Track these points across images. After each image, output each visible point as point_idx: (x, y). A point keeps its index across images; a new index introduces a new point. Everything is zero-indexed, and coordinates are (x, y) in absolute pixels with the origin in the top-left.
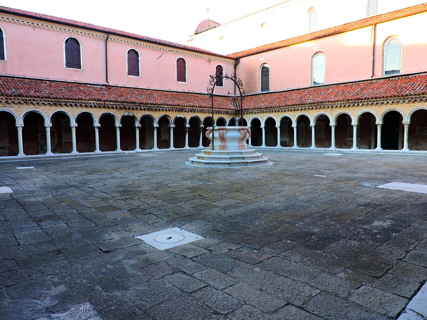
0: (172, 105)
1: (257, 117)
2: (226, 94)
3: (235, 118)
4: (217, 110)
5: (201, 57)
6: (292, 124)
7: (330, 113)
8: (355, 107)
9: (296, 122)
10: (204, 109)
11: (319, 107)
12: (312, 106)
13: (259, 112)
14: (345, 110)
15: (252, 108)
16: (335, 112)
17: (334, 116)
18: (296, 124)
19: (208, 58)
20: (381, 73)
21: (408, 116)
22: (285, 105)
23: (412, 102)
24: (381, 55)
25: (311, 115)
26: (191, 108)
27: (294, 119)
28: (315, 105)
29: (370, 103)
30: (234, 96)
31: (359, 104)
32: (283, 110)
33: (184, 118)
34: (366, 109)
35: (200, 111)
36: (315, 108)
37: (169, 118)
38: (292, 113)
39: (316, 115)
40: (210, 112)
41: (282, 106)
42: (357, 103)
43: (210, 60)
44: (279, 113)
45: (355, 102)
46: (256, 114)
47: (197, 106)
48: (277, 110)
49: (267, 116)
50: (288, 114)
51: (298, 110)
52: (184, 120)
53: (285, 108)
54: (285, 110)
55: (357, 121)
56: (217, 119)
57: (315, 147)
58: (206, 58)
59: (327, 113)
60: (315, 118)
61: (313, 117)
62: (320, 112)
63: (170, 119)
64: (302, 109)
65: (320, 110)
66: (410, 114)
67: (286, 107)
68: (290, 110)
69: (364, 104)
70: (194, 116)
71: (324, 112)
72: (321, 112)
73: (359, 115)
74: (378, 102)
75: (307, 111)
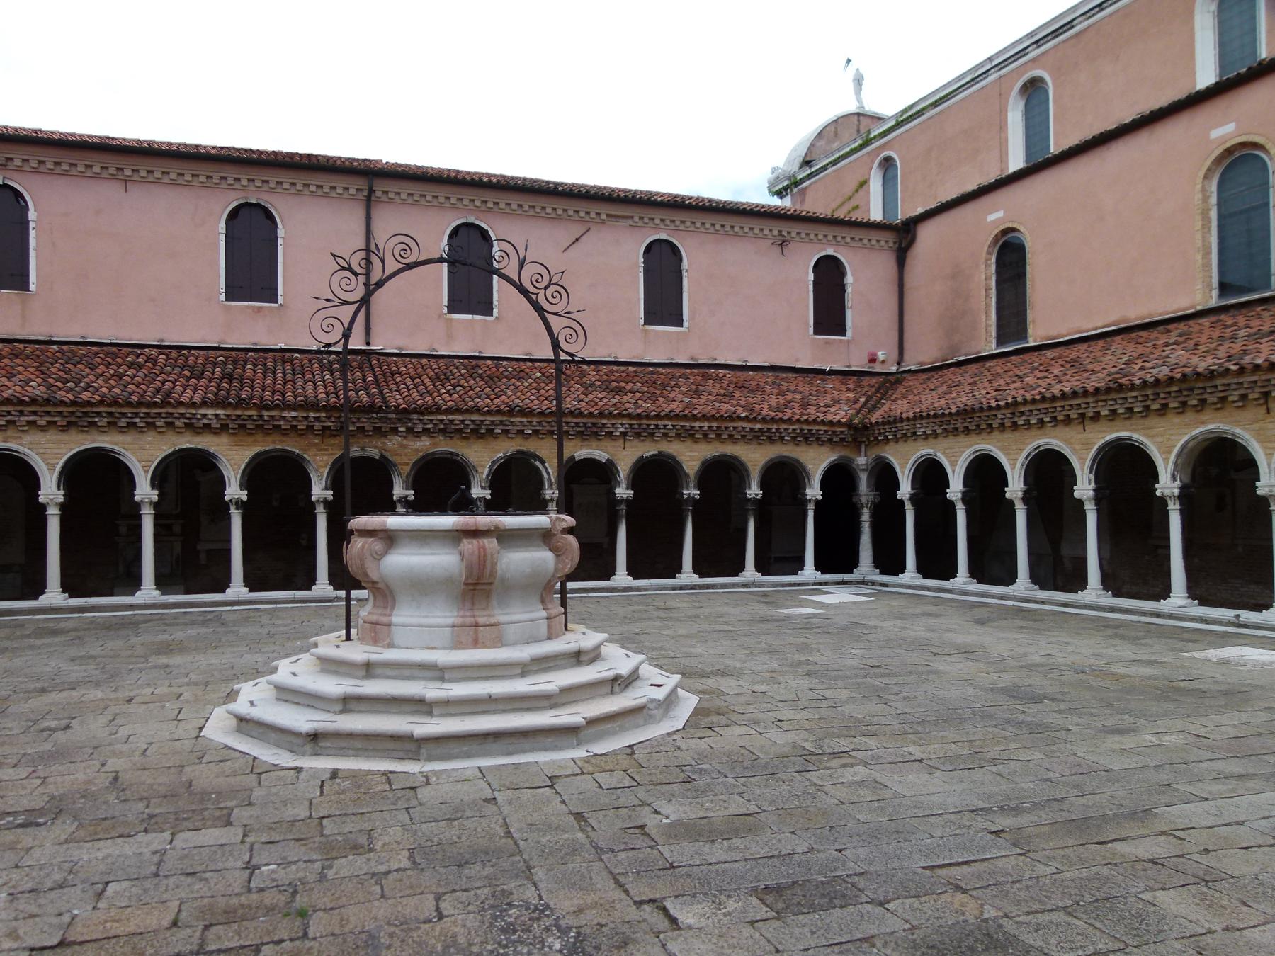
1: (930, 451)
3: (852, 461)
7: (1256, 426)
9: (1092, 477)
10: (697, 424)
11: (1195, 402)
12: (1162, 395)
18: (1093, 484)
25: (1160, 439)
27: (1082, 460)
28: (1175, 389)
36: (1176, 405)
38: (1073, 433)
39: (1182, 442)
44: (1017, 435)
46: (931, 441)
48: (1008, 423)
50: (1053, 440)
51: (1097, 417)
53: (1039, 410)
54: (1041, 422)
56: (763, 462)
59: (1238, 431)
60: (1178, 455)
61: (1170, 452)
62: (1203, 423)
64: (1114, 412)
65: (1204, 417)
67: (1041, 406)
68: (1060, 418)
72: (1210, 427)
75: (1142, 421)
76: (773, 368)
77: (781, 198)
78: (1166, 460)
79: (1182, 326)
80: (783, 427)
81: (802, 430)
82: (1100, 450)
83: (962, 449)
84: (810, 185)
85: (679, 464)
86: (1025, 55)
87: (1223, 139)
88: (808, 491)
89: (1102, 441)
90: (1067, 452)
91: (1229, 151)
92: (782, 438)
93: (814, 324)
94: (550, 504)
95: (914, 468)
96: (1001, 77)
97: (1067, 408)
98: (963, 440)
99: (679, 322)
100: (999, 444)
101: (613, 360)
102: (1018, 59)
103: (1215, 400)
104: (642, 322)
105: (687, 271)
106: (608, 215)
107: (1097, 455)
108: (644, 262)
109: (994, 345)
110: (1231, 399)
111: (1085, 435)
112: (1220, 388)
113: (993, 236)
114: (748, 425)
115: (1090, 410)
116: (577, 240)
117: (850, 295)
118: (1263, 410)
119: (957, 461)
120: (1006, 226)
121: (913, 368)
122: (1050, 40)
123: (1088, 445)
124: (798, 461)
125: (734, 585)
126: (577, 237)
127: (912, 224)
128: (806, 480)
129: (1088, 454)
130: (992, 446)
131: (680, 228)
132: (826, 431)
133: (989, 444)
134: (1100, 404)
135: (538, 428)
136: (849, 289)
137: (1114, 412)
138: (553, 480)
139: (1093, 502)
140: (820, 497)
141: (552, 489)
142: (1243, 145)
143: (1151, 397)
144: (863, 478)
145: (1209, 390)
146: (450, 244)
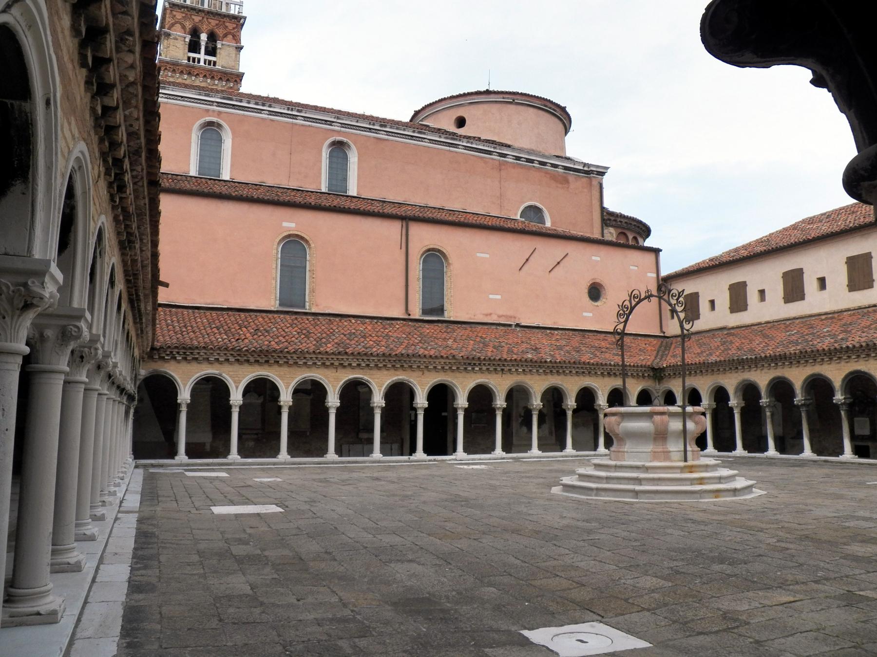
7: (418, 379)
14: (447, 376)
16: (428, 380)
25: (376, 380)
27: (334, 387)
34: (482, 378)
49: (254, 374)
61: (381, 387)
62: (397, 375)
71: (407, 376)
72: (400, 377)
82: (344, 383)
83: (245, 373)
87: (289, 229)
89: (347, 378)
91: (289, 236)
95: (195, 382)
98: (246, 368)
100: (277, 373)
111: (337, 374)
118: (421, 373)
123: (338, 380)
129: (338, 384)
130: (272, 374)
137: (359, 365)
142: (297, 236)
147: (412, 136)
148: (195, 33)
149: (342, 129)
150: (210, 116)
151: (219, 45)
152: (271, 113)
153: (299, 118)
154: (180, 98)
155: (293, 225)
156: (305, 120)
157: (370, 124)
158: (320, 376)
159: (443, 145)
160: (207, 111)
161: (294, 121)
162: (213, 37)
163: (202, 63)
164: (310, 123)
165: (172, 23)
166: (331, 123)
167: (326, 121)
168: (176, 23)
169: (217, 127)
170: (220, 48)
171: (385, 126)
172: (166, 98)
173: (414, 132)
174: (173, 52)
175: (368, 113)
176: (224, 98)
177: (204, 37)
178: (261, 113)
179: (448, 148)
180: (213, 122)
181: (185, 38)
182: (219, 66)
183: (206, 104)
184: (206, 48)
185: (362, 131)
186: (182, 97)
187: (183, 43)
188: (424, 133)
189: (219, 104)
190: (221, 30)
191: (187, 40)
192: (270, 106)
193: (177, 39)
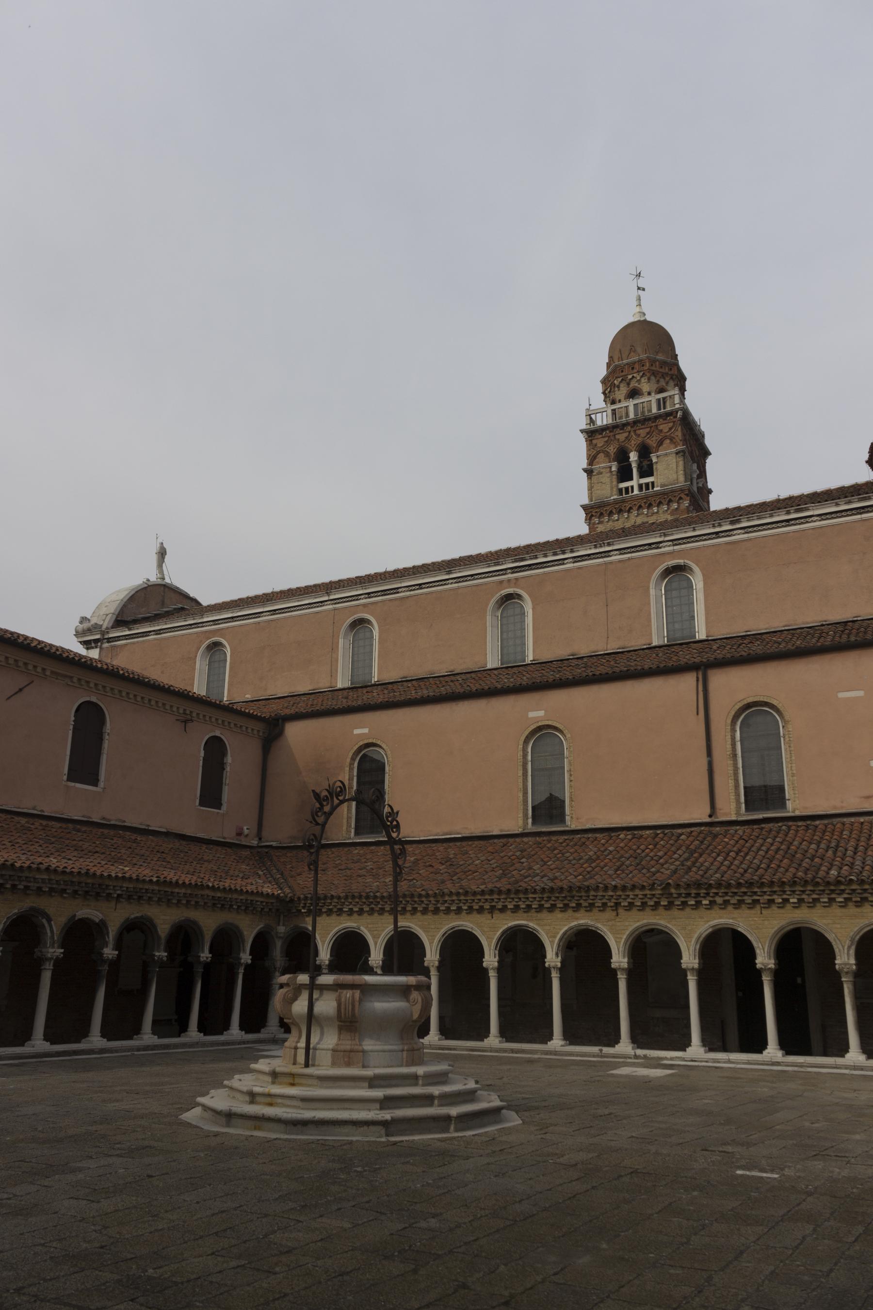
0: (68, 870)
2: (229, 836)
4: (219, 895)
5: (160, 705)
6: (482, 955)
7: (610, 923)
8: (688, 910)
9: (497, 952)
10: (177, 890)
11: (574, 905)
12: (553, 898)
13: (366, 908)
14: (657, 917)
15: (342, 895)
16: (627, 924)
17: (625, 937)
18: (497, 957)
19: (181, 711)
20: (733, 806)
21: (849, 948)
22: (461, 891)
23: (856, 902)
24: (728, 753)
25: (547, 928)
26: (131, 886)
27: (489, 939)
29: (734, 901)
30: (255, 843)
31: (699, 899)
32: (454, 908)
33: (101, 920)
34: (721, 918)
35: (160, 899)
36: (561, 905)
37: (44, 921)
40: (193, 903)
41: (451, 892)
42: (694, 897)
43: (189, 717)
45: (688, 895)
47: (155, 879)
48: (431, 907)
50: (467, 923)
51: (503, 909)
52: (101, 927)
55: (697, 954)
57: (563, 1043)
58: (175, 709)
59: (599, 925)
60: (561, 940)
61: (555, 937)
62: (577, 919)
63: (46, 925)
65: (577, 915)
66: (852, 940)
68: (476, 907)
69: (715, 902)
70: (136, 918)
72: (582, 922)
73: (703, 936)
74: (758, 898)
75: (535, 914)
76: (167, 834)
77: (87, 649)
78: (552, 943)
79: (504, 840)
80: (235, 896)
81: (247, 900)
84: (126, 645)
85: (154, 926)
86: (357, 600)
87: (537, 719)
88: (242, 955)
89: (506, 926)
90: (477, 933)
91: (540, 729)
92: (231, 906)
93: (200, 795)
94: (48, 963)
96: (335, 609)
97: (483, 901)
99: (95, 783)
100: (420, 923)
101: (39, 813)
102: (351, 601)
103: (587, 905)
104: (65, 778)
105: (108, 734)
106: (52, 672)
107: (501, 936)
108: (74, 721)
109: (352, 834)
110: (596, 905)
111: (493, 921)
112: (591, 897)
113: (357, 746)
114: (211, 894)
115: (499, 903)
116: (21, 690)
117: (228, 774)
118: (614, 913)
119: (380, 935)
120: (370, 741)
121: (274, 844)
122: (379, 596)
124: (237, 927)
125: (176, 1046)
126: (21, 687)
127: (280, 721)
128: (241, 945)
129: (495, 934)
131: (108, 694)
132: (262, 902)
133: (410, 922)
134: (509, 900)
135: (54, 886)
136: (228, 769)
138: (56, 938)
139: (496, 971)
140: (249, 962)
141: (53, 947)
143: (545, 899)
144: (279, 944)
145: (584, 898)
146: (75, 716)
147: (788, 521)
148: (622, 457)
149: (676, 547)
150: (505, 589)
151: (654, 460)
152: (577, 559)
153: (612, 553)
154: (469, 578)
155: (541, 713)
156: (621, 554)
157: (714, 526)
158: (471, 925)
159: (848, 515)
160: (501, 582)
161: (606, 559)
162: (645, 452)
163: (636, 492)
164: (629, 555)
165: (593, 456)
166: (657, 545)
167: (650, 544)
168: (598, 453)
169: (518, 598)
170: (656, 463)
171: (738, 521)
172: (456, 583)
173: (788, 513)
174: (598, 492)
175: (784, 495)
176: (516, 561)
177: (633, 457)
178: (563, 564)
179: (859, 517)
180: (511, 594)
181: (611, 467)
182: (658, 486)
183: (499, 575)
184: (640, 468)
185: (705, 540)
186: (472, 575)
187: (609, 474)
188: (807, 509)
189: (514, 570)
190: (654, 438)
191: (614, 469)
192: (572, 551)
193: (601, 473)
